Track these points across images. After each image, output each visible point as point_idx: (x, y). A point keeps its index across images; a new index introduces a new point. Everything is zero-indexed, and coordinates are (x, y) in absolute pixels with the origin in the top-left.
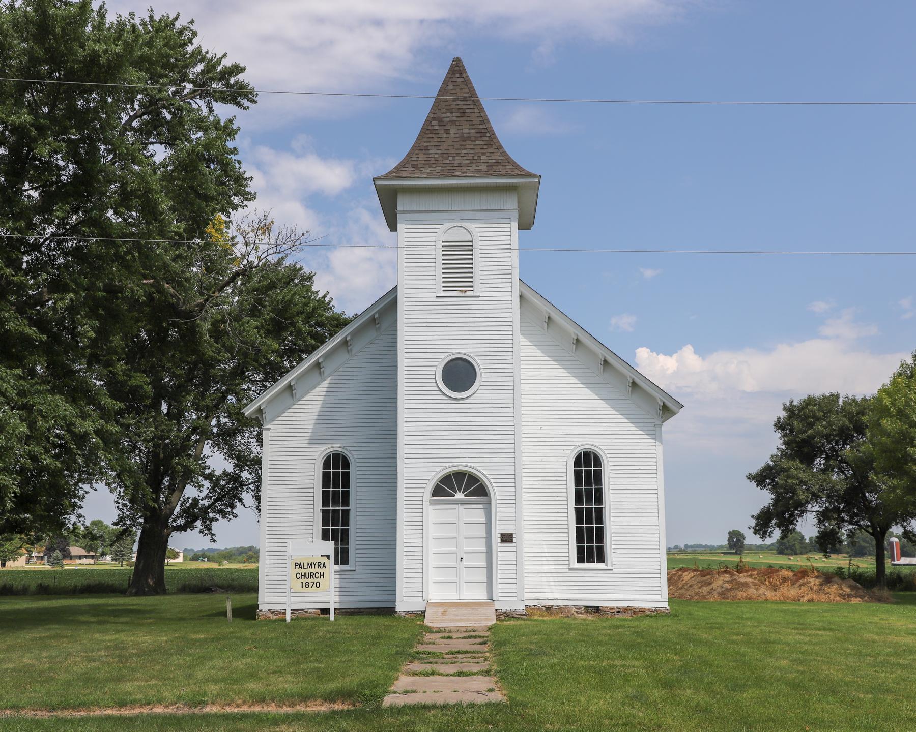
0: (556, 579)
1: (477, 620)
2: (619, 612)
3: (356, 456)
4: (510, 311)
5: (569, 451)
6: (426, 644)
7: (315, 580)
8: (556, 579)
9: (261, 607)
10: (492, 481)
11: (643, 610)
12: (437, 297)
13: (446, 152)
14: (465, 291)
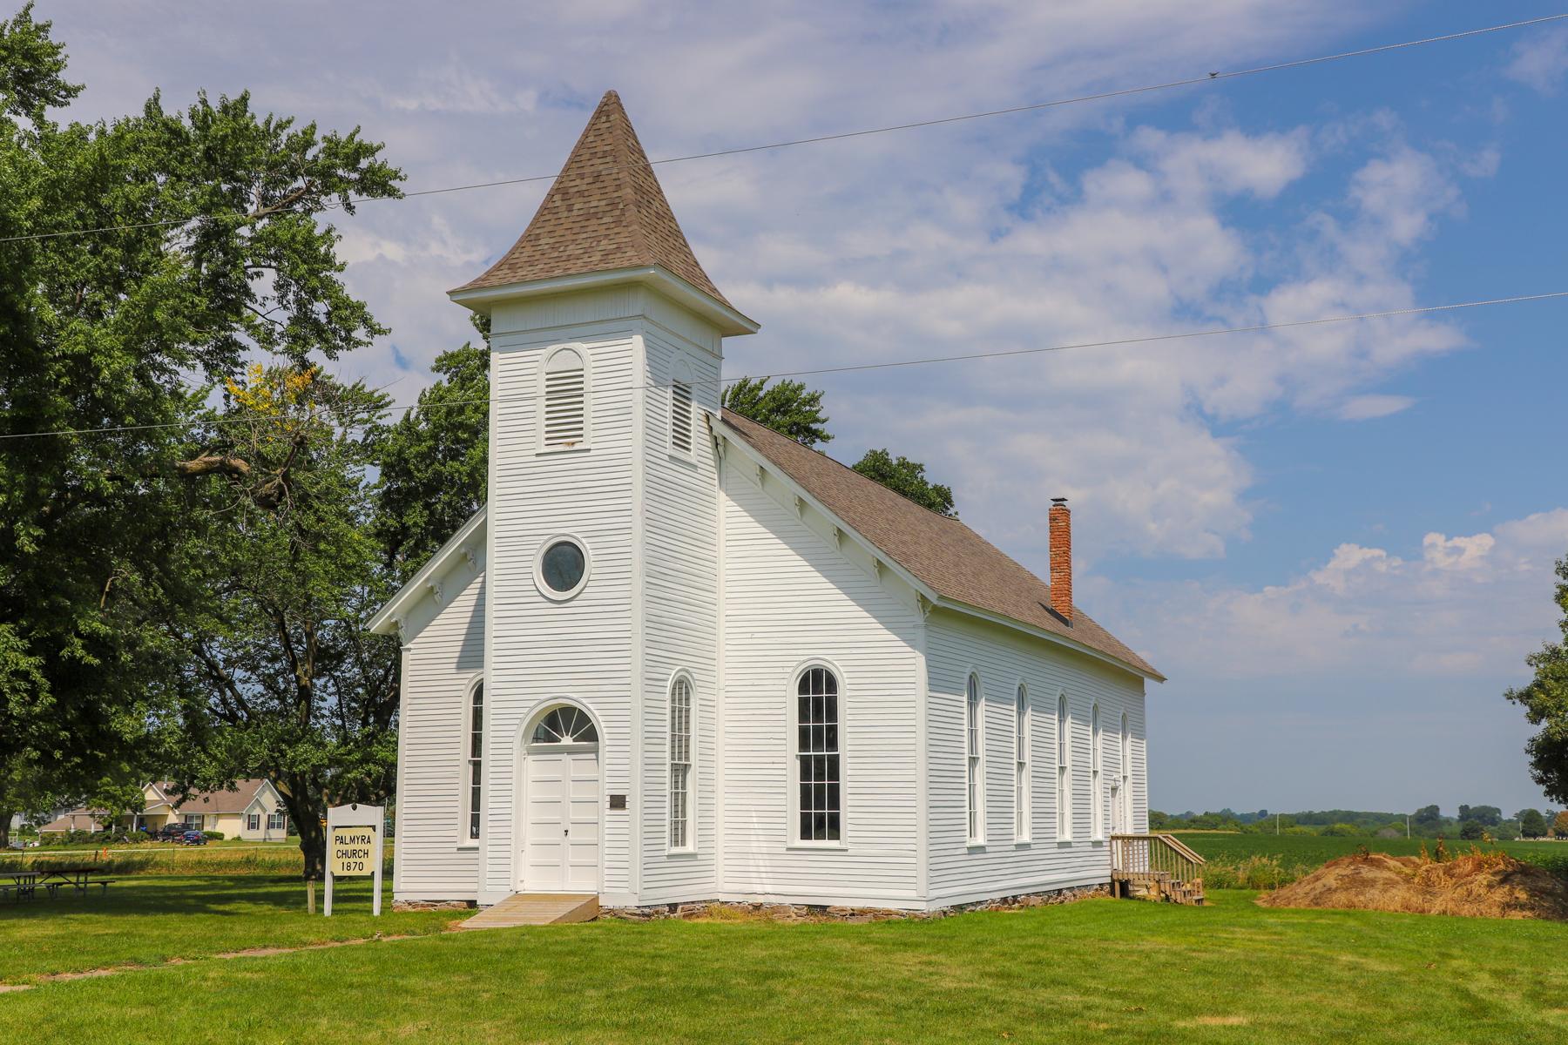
0: (767, 863)
2: (853, 915)
3: (845, 675)
5: (790, 670)
7: (358, 860)
8: (767, 863)
9: (396, 897)
11: (889, 913)
14: (573, 444)
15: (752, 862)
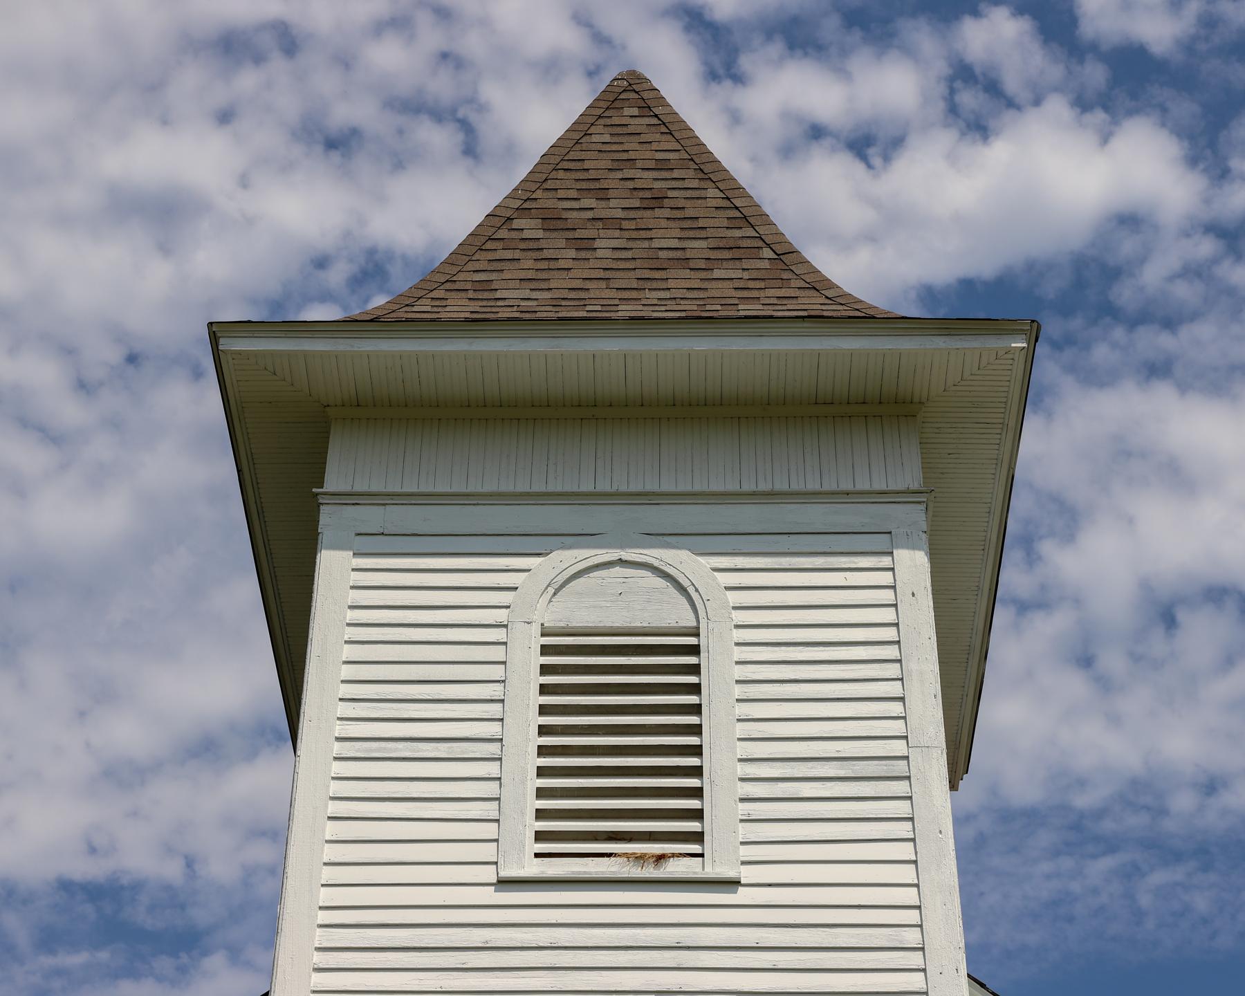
4: (915, 959)
12: (504, 883)
13: (572, 295)
14: (661, 858)
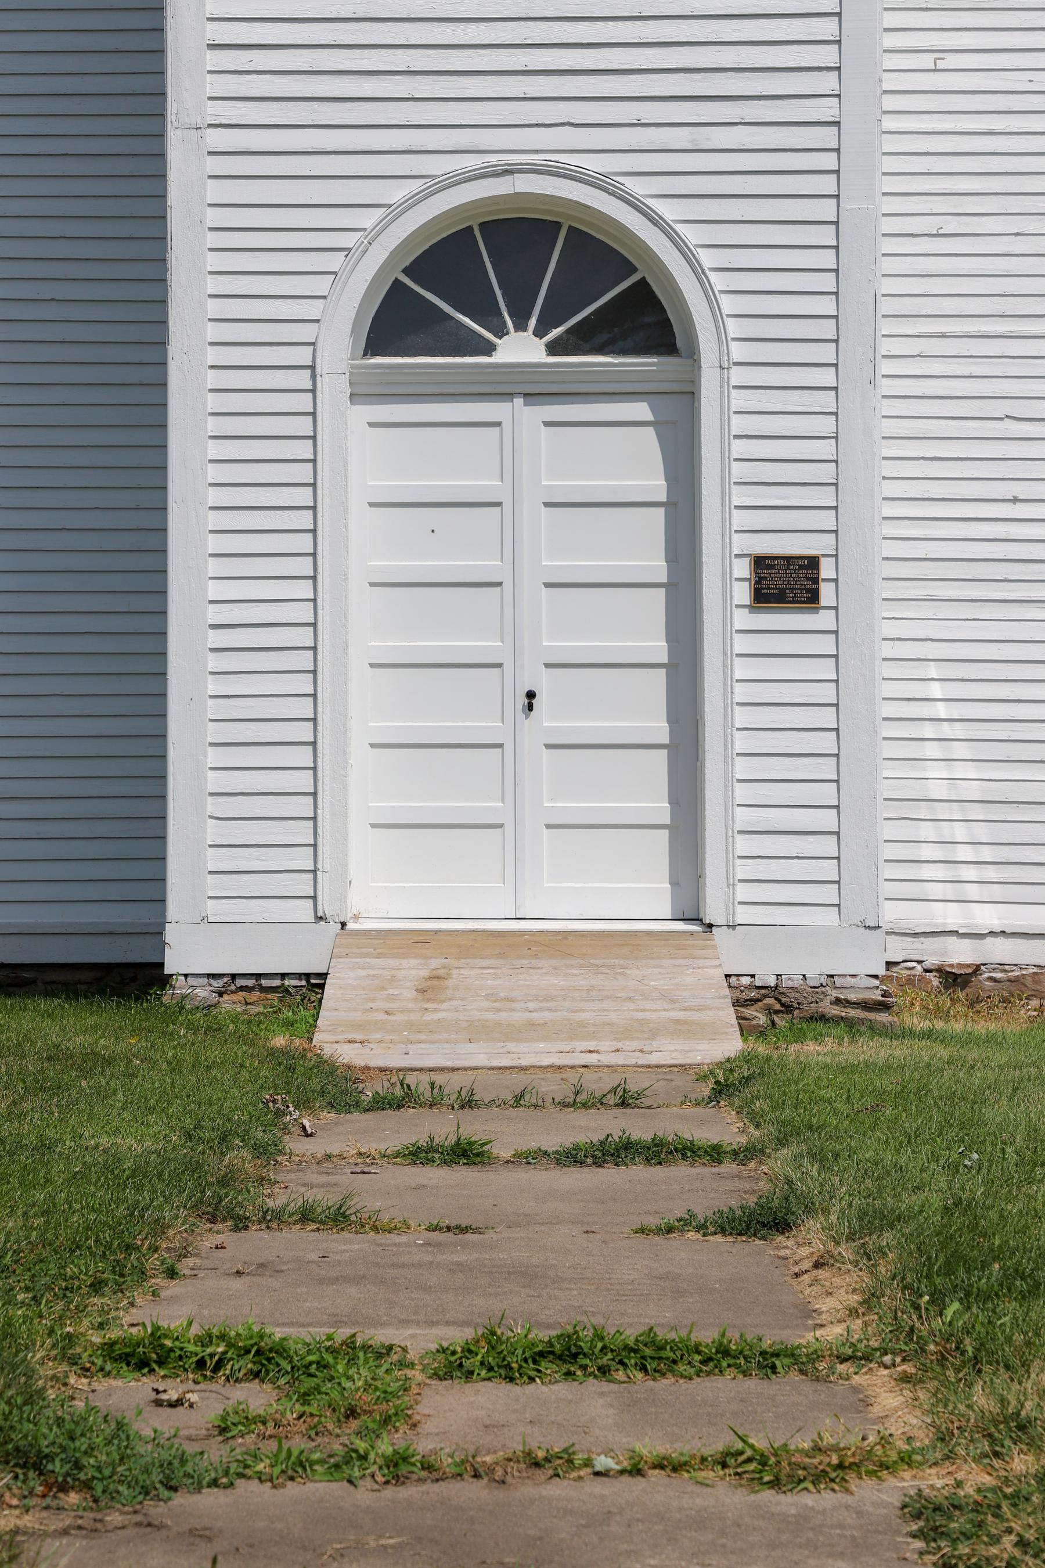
0: (982, 833)
1: (627, 1032)
6: (272, 1219)
8: (982, 833)
10: (707, 259)
15: (927, 831)
